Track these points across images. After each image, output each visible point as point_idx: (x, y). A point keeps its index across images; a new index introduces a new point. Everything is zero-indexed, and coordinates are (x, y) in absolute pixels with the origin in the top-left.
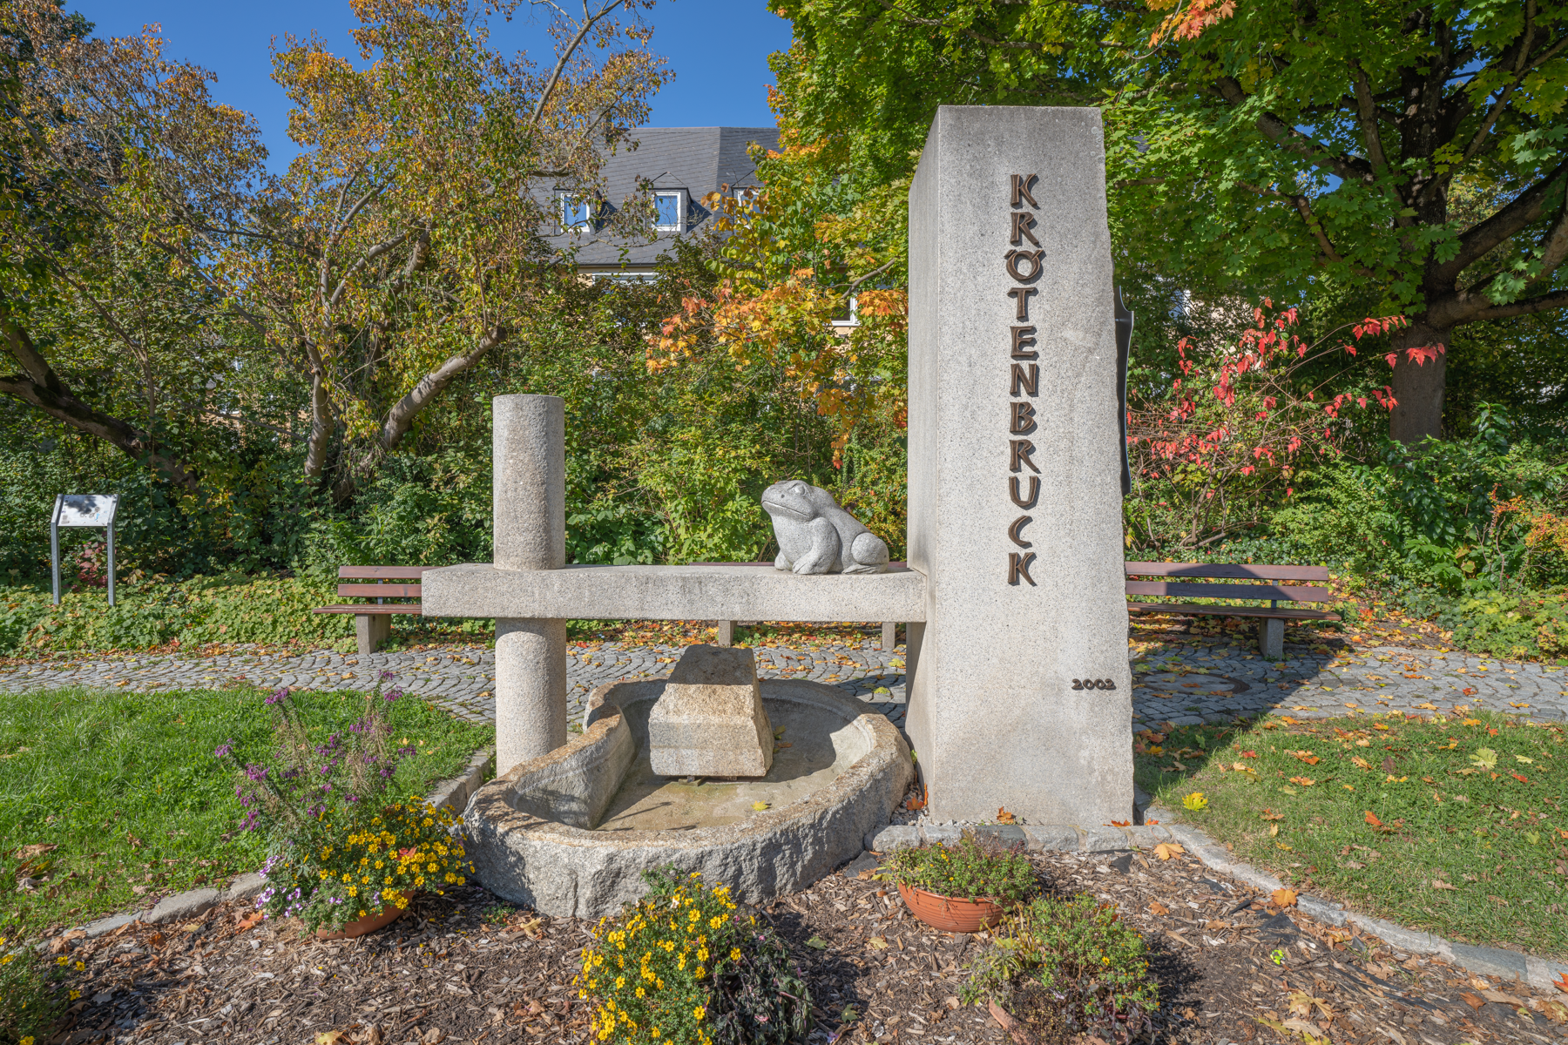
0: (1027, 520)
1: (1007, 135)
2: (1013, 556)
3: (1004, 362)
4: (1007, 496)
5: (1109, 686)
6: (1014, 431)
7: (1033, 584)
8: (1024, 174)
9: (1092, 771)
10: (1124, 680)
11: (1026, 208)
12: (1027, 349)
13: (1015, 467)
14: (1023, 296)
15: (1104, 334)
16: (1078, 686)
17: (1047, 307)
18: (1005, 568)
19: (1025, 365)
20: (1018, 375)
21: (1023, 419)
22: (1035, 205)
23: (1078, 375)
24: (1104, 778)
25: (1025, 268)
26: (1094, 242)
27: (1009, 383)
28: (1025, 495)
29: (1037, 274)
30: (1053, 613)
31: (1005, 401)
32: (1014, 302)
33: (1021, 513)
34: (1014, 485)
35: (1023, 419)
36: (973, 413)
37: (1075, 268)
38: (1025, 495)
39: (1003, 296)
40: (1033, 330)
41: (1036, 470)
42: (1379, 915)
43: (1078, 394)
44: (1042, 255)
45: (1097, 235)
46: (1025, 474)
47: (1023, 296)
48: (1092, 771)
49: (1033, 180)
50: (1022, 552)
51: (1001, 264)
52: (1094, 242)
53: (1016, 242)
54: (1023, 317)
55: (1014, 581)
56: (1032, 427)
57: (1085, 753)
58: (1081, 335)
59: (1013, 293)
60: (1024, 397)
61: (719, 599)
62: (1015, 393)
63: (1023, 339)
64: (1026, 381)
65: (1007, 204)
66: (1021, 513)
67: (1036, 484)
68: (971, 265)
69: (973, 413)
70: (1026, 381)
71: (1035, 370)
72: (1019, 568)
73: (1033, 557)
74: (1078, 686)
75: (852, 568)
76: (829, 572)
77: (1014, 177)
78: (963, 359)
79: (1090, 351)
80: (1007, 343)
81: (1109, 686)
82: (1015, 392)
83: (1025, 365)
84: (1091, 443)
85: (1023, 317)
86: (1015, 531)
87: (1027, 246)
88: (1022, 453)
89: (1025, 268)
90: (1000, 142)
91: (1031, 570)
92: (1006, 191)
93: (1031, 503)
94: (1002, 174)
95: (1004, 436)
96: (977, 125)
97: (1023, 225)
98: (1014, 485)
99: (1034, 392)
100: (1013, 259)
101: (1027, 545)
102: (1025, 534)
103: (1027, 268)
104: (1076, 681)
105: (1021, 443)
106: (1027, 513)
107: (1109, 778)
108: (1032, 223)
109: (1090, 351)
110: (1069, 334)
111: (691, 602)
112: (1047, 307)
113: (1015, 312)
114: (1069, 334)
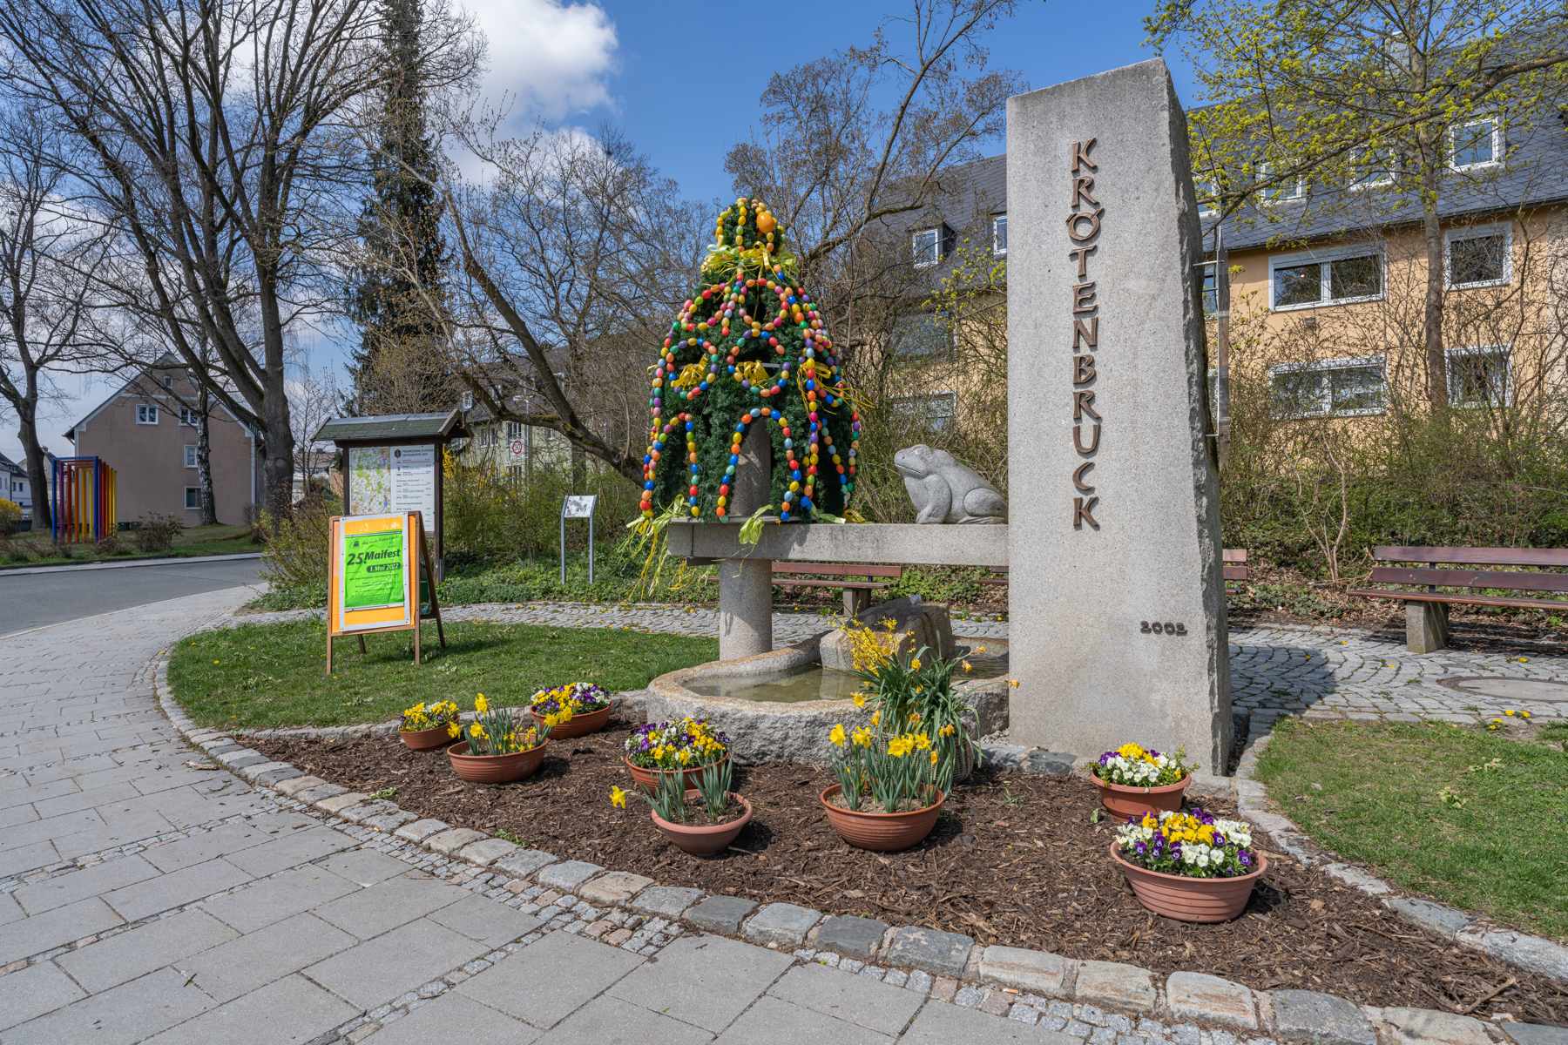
0: (1087, 467)
1: (1068, 109)
2: (1079, 502)
5: (1181, 630)
6: (1076, 384)
7: (1096, 527)
9: (1165, 716)
11: (1085, 174)
12: (1087, 306)
13: (1078, 419)
15: (1169, 279)
16: (1145, 628)
18: (1070, 513)
19: (1087, 322)
21: (1085, 371)
22: (1094, 169)
23: (1142, 323)
24: (1178, 725)
25: (1084, 230)
26: (1157, 190)
27: (1072, 339)
28: (1087, 443)
29: (1096, 233)
30: (1119, 556)
31: (1068, 356)
34: (1077, 431)
35: (1085, 371)
36: (1040, 370)
37: (1138, 220)
41: (1099, 418)
42: (1506, 921)
43: (1142, 342)
44: (1100, 214)
45: (1160, 183)
46: (1087, 424)
48: (1165, 716)
52: (1157, 190)
54: (1082, 276)
55: (1078, 526)
56: (1092, 378)
57: (1157, 697)
58: (1144, 282)
59: (1074, 255)
60: (1085, 350)
62: (1076, 348)
63: (1085, 295)
65: (1069, 174)
66: (1083, 461)
67: (1098, 431)
68: (1036, 236)
69: (1040, 370)
71: (1096, 324)
72: (1083, 513)
73: (1094, 501)
74: (1145, 628)
75: (967, 518)
76: (944, 522)
78: (1030, 323)
79: (1154, 298)
80: (1069, 303)
83: (1087, 322)
84: (1156, 387)
85: (1082, 276)
87: (1086, 209)
88: (1084, 402)
89: (1084, 230)
90: (1062, 116)
92: (1068, 161)
93: (1093, 451)
95: (1067, 389)
96: (1040, 108)
97: (1083, 188)
98: (1077, 431)
99: (1093, 347)
100: (1075, 221)
101: (1090, 490)
102: (1088, 480)
105: (1082, 395)
107: (1184, 725)
108: (1090, 187)
110: (1132, 284)
111: (836, 546)
113: (1077, 272)
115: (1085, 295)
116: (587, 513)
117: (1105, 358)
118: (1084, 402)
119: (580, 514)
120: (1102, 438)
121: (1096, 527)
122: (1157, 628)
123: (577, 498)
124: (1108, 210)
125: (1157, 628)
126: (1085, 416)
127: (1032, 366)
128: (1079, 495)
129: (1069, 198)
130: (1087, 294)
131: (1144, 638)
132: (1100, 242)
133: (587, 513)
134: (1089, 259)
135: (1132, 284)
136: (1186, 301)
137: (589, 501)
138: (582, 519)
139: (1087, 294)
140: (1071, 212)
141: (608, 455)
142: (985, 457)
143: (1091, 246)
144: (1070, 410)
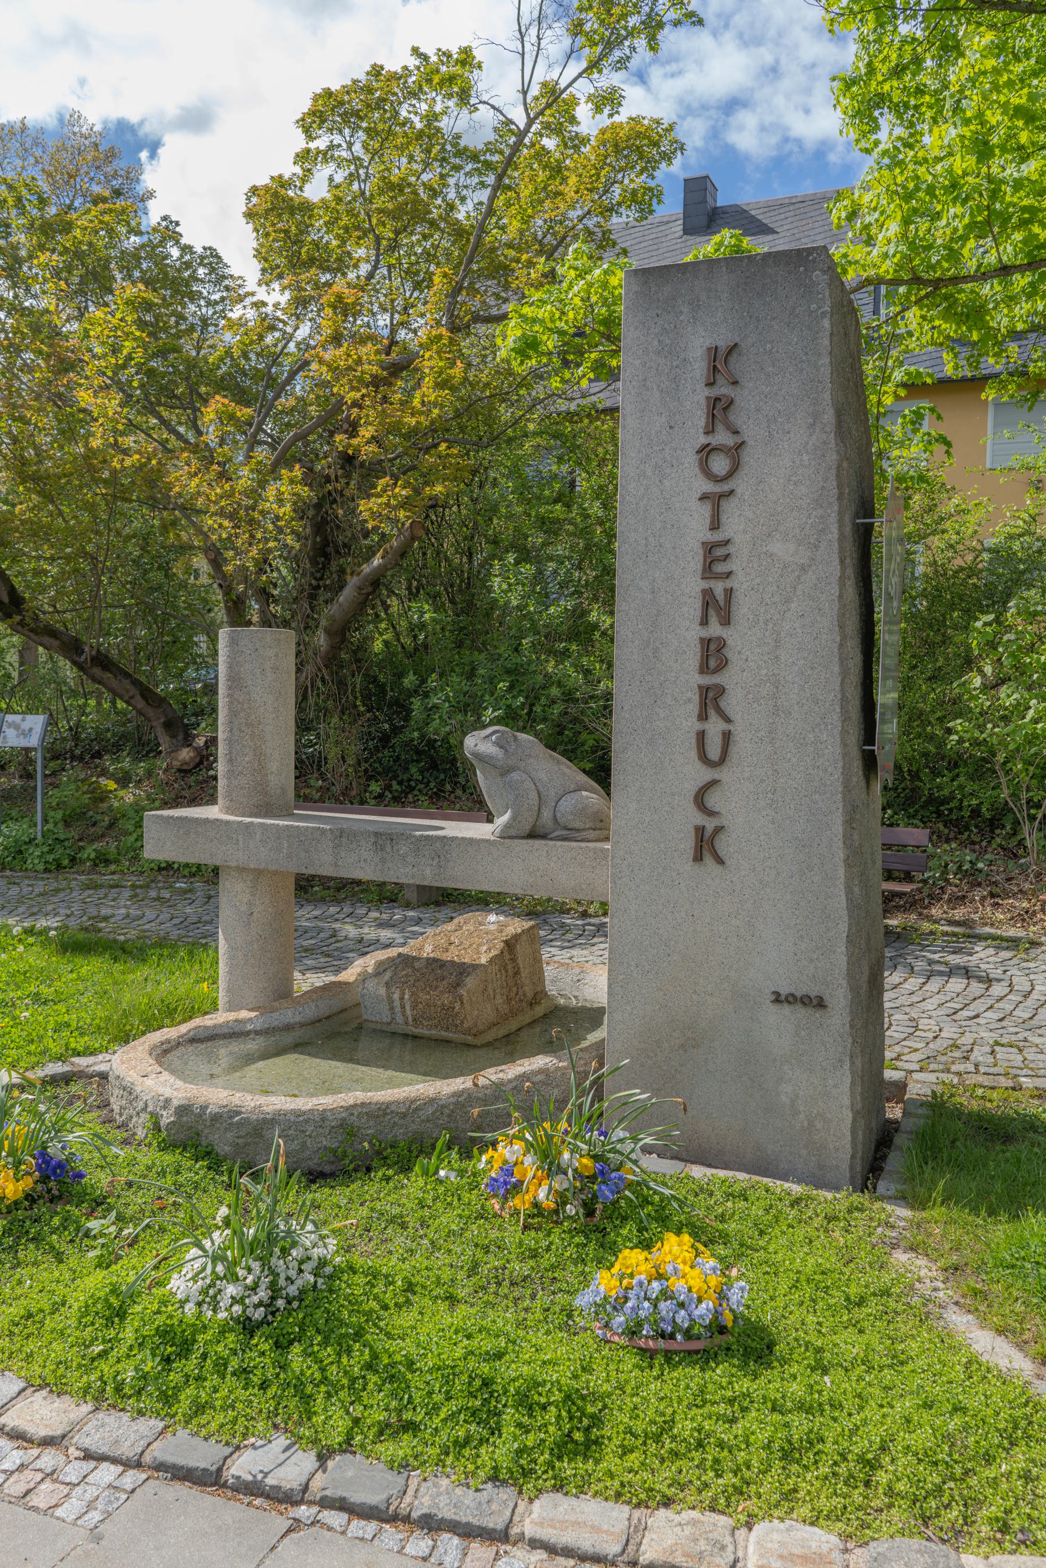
0: (713, 783)
2: (700, 831)
4: (693, 754)
5: (820, 1004)
7: (720, 861)
8: (723, 344)
12: (720, 568)
13: (703, 717)
14: (716, 501)
17: (749, 514)
18: (688, 844)
19: (719, 588)
20: (708, 600)
23: (788, 601)
24: (811, 1124)
25: (720, 465)
27: (699, 613)
28: (714, 753)
31: (694, 633)
32: (705, 510)
33: (706, 775)
34: (701, 736)
35: (713, 655)
36: (656, 650)
41: (728, 720)
47: (716, 501)
49: (733, 349)
50: (710, 824)
51: (691, 460)
52: (812, 425)
53: (710, 431)
55: (698, 858)
59: (704, 497)
60: (715, 629)
63: (714, 556)
65: (700, 386)
66: (706, 775)
71: (729, 593)
72: (705, 845)
73: (718, 830)
79: (803, 569)
80: (696, 563)
81: (820, 1004)
82: (704, 622)
86: (700, 799)
87: (722, 437)
88: (711, 700)
91: (725, 845)
92: (699, 368)
94: (697, 345)
97: (719, 410)
98: (701, 736)
100: (706, 452)
104: (777, 994)
106: (717, 777)
107: (819, 1125)
109: (803, 569)
110: (777, 547)
111: (383, 860)
112: (749, 514)
115: (714, 556)
116: (34, 741)
117: (741, 638)
118: (711, 700)
119: (23, 743)
120: (733, 750)
121: (720, 861)
122: (791, 999)
123: (17, 718)
124: (751, 442)
125: (791, 999)
126: (712, 713)
128: (700, 819)
129: (700, 420)
130: (719, 552)
131: (774, 1008)
132: (742, 484)
133: (34, 741)
134: (724, 503)
135: (777, 547)
136: (842, 579)
137: (36, 722)
138: (27, 750)
139: (719, 552)
141: (72, 648)
142: (586, 745)
143: (726, 487)
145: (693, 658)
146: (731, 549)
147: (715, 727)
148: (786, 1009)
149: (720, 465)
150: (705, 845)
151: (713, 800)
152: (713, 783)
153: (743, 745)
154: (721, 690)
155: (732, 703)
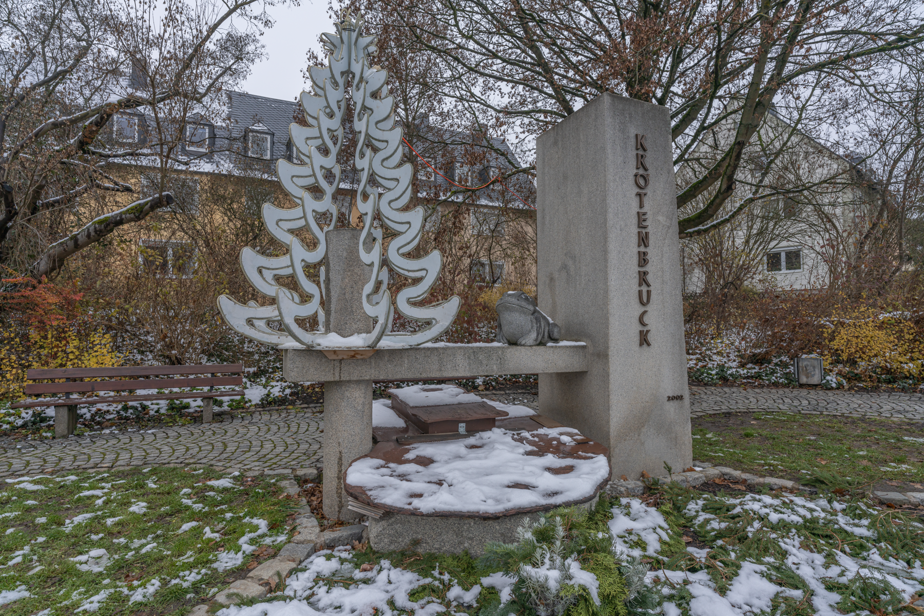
0: (645, 312)
2: (641, 332)
3: (634, 230)
4: (637, 300)
7: (649, 345)
8: (640, 133)
10: (687, 394)
13: (640, 285)
18: (637, 339)
21: (643, 260)
28: (645, 300)
32: (638, 199)
33: (643, 309)
34: (640, 292)
35: (643, 260)
38: (645, 300)
39: (633, 196)
40: (644, 214)
41: (649, 285)
51: (632, 178)
54: (641, 206)
55: (641, 344)
60: (642, 249)
61: (485, 362)
63: (641, 218)
64: (643, 240)
65: (634, 148)
66: (643, 309)
67: (649, 292)
70: (643, 240)
72: (644, 340)
73: (648, 331)
77: (637, 135)
78: (618, 227)
79: (669, 227)
80: (635, 221)
81: (680, 398)
82: (639, 246)
83: (644, 231)
85: (641, 206)
87: (641, 172)
88: (643, 279)
92: (633, 142)
94: (633, 131)
95: (634, 269)
103: (642, 181)
109: (669, 227)
110: (660, 218)
114: (660, 218)
118: (643, 279)
127: (619, 252)
128: (641, 328)
132: (649, 191)
140: (635, 171)
144: (636, 281)
145: (635, 260)
146: (646, 217)
147: (644, 289)
148: (671, 403)
149: (642, 182)
150: (644, 340)
151: (646, 319)
152: (645, 312)
153: (653, 296)
154: (645, 273)
155: (650, 278)
